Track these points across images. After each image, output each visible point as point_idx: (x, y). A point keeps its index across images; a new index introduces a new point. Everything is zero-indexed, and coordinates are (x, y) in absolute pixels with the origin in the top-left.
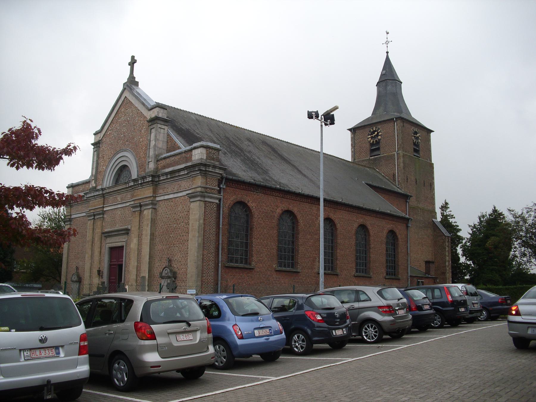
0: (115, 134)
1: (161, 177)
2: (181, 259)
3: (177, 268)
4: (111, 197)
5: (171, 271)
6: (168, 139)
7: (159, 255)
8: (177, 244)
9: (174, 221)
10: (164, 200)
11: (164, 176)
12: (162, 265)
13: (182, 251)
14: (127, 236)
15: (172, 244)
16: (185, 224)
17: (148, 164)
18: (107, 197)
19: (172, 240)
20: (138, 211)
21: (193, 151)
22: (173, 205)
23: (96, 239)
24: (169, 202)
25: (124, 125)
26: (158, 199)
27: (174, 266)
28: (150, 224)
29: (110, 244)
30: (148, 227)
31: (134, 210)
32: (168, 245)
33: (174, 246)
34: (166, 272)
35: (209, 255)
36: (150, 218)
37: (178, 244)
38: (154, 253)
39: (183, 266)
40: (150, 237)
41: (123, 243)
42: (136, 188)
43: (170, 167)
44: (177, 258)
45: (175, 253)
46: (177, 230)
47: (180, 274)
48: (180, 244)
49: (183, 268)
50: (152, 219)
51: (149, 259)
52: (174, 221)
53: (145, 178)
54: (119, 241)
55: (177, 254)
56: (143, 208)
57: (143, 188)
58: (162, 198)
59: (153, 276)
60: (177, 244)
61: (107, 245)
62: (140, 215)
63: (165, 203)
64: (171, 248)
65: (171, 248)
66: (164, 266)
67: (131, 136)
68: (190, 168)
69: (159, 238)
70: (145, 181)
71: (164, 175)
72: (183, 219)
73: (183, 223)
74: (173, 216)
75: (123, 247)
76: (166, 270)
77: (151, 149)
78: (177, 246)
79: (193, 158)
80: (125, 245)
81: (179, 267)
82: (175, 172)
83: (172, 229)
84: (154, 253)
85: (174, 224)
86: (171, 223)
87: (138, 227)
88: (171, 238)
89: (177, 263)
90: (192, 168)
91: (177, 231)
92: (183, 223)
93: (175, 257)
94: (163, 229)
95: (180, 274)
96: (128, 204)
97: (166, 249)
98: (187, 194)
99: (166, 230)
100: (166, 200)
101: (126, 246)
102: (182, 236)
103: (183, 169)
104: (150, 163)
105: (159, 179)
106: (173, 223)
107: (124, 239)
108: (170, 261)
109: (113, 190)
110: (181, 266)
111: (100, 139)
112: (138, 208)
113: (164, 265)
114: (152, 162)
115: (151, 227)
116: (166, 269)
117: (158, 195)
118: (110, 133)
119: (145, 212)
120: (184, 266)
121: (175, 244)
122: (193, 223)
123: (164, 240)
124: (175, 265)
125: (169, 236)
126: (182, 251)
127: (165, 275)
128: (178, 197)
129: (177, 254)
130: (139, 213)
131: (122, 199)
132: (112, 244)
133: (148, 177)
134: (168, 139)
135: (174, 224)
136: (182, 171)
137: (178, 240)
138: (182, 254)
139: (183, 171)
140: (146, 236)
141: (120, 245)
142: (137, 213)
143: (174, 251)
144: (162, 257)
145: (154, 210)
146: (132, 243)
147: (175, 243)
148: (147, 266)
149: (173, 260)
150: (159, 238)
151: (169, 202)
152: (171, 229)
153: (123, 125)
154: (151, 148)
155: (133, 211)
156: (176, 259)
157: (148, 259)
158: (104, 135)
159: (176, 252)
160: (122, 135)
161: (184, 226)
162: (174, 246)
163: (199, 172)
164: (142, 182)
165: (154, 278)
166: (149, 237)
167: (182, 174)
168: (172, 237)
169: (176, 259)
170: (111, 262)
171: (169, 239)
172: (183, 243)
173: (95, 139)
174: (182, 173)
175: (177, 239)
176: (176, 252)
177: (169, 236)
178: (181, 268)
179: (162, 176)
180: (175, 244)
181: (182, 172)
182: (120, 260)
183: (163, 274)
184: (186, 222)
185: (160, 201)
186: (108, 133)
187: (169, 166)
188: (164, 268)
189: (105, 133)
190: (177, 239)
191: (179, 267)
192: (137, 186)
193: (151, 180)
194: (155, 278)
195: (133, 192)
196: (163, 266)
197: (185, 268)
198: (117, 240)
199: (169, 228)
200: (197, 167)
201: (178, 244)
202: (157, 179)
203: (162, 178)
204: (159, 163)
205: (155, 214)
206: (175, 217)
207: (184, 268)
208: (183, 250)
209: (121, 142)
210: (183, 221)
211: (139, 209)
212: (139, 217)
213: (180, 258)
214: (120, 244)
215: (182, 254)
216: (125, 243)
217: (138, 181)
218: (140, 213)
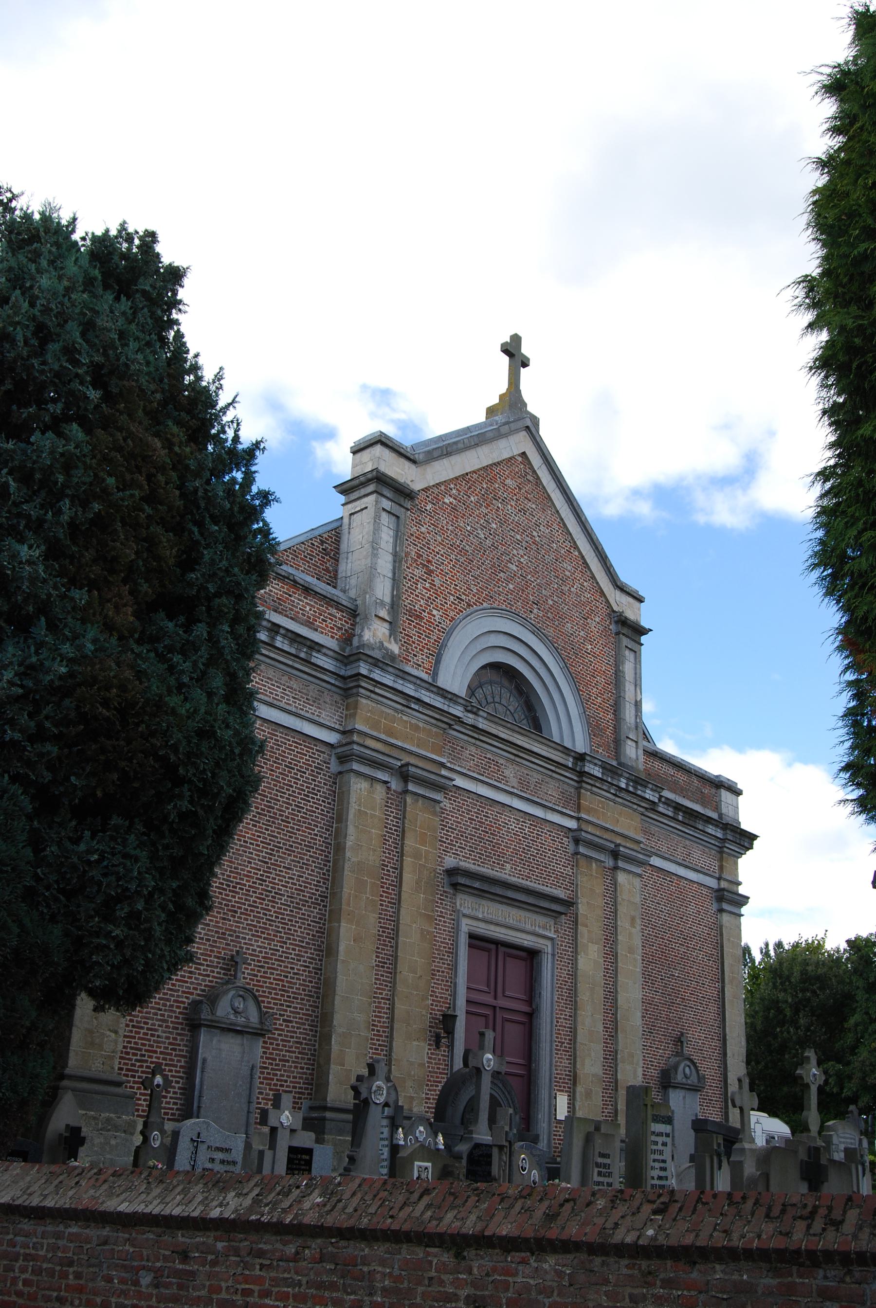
4: (473, 749)
18: (456, 738)
25: (518, 537)
29: (482, 925)
41: (541, 941)
42: (594, 789)
53: (641, 785)
70: (639, 792)
71: (668, 805)
82: (696, 817)
109: (511, 739)
128: (686, 879)
132: (492, 928)
133: (652, 790)
136: (712, 824)
167: (710, 831)
174: (710, 830)
192: (605, 788)
217: (616, 777)
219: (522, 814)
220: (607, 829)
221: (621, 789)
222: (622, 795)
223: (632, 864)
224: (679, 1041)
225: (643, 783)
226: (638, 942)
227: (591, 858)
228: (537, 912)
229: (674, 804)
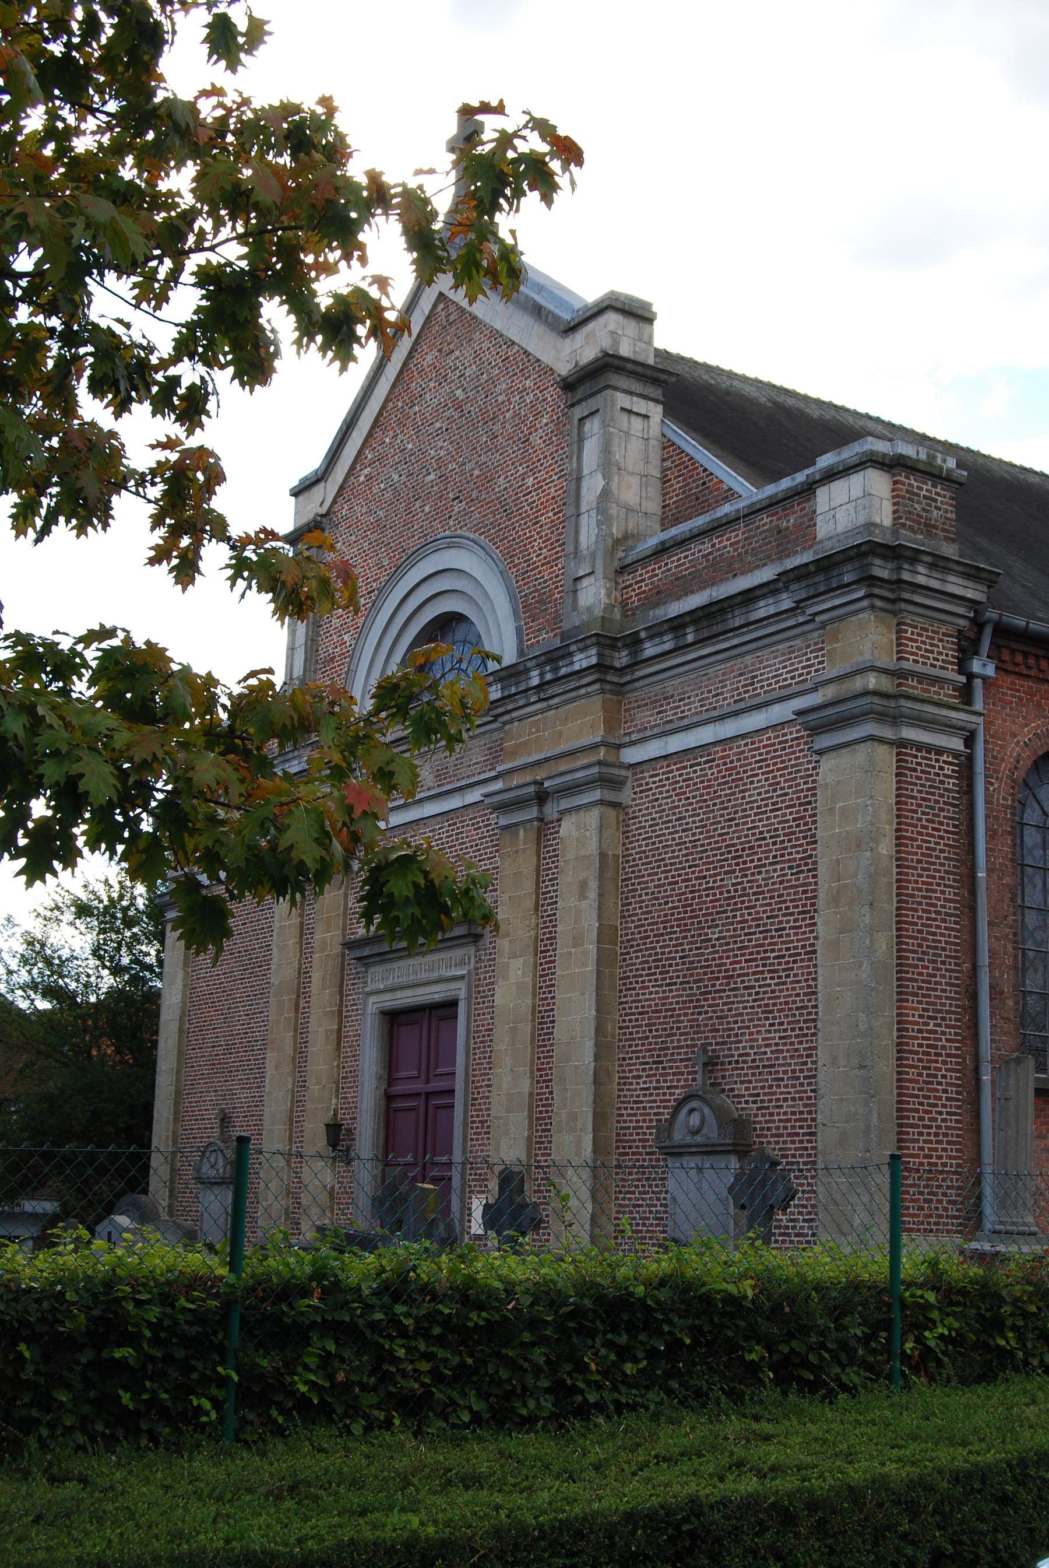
0: (396, 477)
1: (647, 645)
2: (772, 1052)
3: (754, 1102)
5: (723, 1117)
6: (668, 464)
7: (647, 1038)
8: (747, 974)
9: (726, 860)
10: (665, 757)
11: (665, 638)
12: (668, 1088)
13: (779, 1011)
14: (471, 950)
15: (718, 978)
16: (790, 868)
17: (575, 591)
19: (721, 958)
20: (528, 826)
21: (819, 492)
22: (716, 779)
23: (316, 976)
24: (692, 766)
25: (438, 425)
26: (632, 755)
27: (732, 1090)
28: (593, 885)
29: (388, 996)
30: (583, 896)
31: (504, 821)
32: (695, 982)
33: (728, 984)
34: (695, 1120)
35: (931, 1027)
36: (596, 853)
37: (754, 973)
38: (621, 1028)
39: (786, 1086)
40: (598, 949)
41: (453, 985)
42: (515, 714)
43: (692, 592)
44: (752, 1047)
45: (736, 1022)
46: (743, 902)
47: (769, 1129)
48: (762, 972)
49: (785, 1100)
50: (603, 856)
51: (597, 1058)
52: (726, 860)
53: (563, 657)
54: (435, 975)
55: (748, 1027)
56: (551, 810)
57: (550, 708)
58: (653, 749)
59: (618, 1148)
60: (747, 974)
61: (373, 999)
62: (538, 843)
63: (672, 771)
64: (714, 999)
65: (714, 999)
66: (678, 1091)
67: (476, 472)
68: (809, 575)
69: (647, 949)
70: (563, 671)
71: (660, 634)
72: (774, 843)
73: (776, 863)
74: (720, 835)
75: (450, 1006)
76: (692, 1110)
77: (584, 519)
78: (745, 988)
79: (823, 529)
80: (462, 995)
81: (765, 1094)
82: (723, 611)
83: (719, 900)
84: (621, 1028)
85: (726, 873)
86: (708, 870)
87: (530, 903)
88: (714, 946)
89: (753, 1075)
90: (821, 578)
91: (747, 908)
92: (778, 867)
93: (740, 1042)
94: (666, 903)
95: (769, 1129)
96: (474, 796)
97: (684, 1002)
98: (800, 713)
99: (684, 906)
100: (675, 759)
101: (469, 998)
102: (776, 930)
103: (768, 589)
104: (585, 582)
105: (634, 654)
106: (722, 867)
107: (462, 963)
108: (711, 1064)
110: (778, 1086)
111: (324, 510)
112: (529, 806)
113: (676, 1087)
114: (592, 579)
115: (601, 895)
116: (694, 1104)
117: (634, 737)
118: (369, 478)
119: (567, 827)
120: (794, 1086)
121: (739, 976)
122: (838, 862)
123: (674, 958)
124: (742, 1082)
125: (700, 935)
126: (779, 1011)
127: (688, 1139)
128: (743, 736)
129: (748, 1027)
130: (533, 836)
131: (440, 775)
132: (399, 994)
133: (581, 650)
134: (668, 464)
135: (726, 873)
136: (764, 596)
137: (751, 954)
138: (781, 1024)
139: (771, 601)
140: (577, 940)
141: (437, 997)
142: (521, 833)
143: (730, 1010)
144: (668, 1048)
145: (611, 813)
146: (501, 982)
147: (734, 970)
148: (587, 1095)
149: (727, 1056)
150: (647, 949)
151: (692, 766)
152: (711, 901)
153: (431, 429)
154: (583, 509)
155: (504, 828)
156: (748, 1055)
157: (592, 1059)
158: (342, 488)
159: (741, 1015)
160: (432, 477)
161: (781, 882)
162: (728, 984)
163: (861, 594)
164: (549, 677)
165: (620, 1154)
166: (592, 948)
167: (761, 613)
168: (718, 939)
169: (748, 1055)
170: (391, 1081)
171: (703, 954)
172: (784, 970)
173: (297, 513)
174: (764, 609)
175: (745, 947)
176: (741, 1015)
177: (700, 935)
178: (778, 1100)
179: (651, 637)
180: (739, 976)
181: (762, 603)
182: (441, 1070)
183: (679, 1135)
184: (794, 860)
185: (645, 767)
186: (362, 479)
187: (683, 586)
188: (681, 1103)
189: (345, 481)
190: (745, 947)
191: (765, 1094)
192: (521, 703)
193: (594, 660)
194: (627, 1154)
195: (496, 736)
196: (671, 1094)
197: (801, 1099)
198: (423, 976)
199: (700, 897)
200: (849, 567)
201: (754, 973)
202: (622, 659)
203: (650, 650)
204: (628, 579)
205: (618, 829)
206: (732, 839)
207: (793, 1099)
208: (787, 1003)
209: (427, 509)
210: (775, 857)
211: (533, 812)
212: (533, 851)
213: (767, 1046)
214: (435, 994)
215: (781, 1024)
216: (462, 985)
217: (523, 677)
218: (539, 831)
219: (439, 818)
220: (538, 763)
221: (539, 687)
222: (550, 692)
223: (581, 792)
224: (711, 1064)
225: (560, 653)
226: (591, 923)
227: (516, 824)
228: (450, 947)
229: (666, 627)
